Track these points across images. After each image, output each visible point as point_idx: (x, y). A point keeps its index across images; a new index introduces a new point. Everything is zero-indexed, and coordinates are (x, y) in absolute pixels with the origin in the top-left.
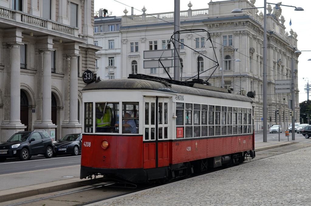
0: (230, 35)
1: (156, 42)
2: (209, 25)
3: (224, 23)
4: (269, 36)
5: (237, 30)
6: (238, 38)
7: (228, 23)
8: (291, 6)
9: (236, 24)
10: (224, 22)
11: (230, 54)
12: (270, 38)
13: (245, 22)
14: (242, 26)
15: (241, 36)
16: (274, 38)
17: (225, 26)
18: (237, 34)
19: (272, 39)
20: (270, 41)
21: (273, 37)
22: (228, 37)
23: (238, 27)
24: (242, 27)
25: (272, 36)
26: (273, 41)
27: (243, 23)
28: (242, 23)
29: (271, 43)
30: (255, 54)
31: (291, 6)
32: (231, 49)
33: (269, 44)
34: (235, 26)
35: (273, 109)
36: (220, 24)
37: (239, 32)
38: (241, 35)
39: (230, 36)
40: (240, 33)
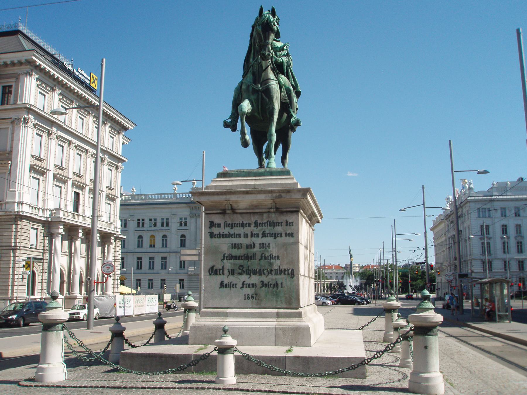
1: (143, 220)
2: (191, 207)
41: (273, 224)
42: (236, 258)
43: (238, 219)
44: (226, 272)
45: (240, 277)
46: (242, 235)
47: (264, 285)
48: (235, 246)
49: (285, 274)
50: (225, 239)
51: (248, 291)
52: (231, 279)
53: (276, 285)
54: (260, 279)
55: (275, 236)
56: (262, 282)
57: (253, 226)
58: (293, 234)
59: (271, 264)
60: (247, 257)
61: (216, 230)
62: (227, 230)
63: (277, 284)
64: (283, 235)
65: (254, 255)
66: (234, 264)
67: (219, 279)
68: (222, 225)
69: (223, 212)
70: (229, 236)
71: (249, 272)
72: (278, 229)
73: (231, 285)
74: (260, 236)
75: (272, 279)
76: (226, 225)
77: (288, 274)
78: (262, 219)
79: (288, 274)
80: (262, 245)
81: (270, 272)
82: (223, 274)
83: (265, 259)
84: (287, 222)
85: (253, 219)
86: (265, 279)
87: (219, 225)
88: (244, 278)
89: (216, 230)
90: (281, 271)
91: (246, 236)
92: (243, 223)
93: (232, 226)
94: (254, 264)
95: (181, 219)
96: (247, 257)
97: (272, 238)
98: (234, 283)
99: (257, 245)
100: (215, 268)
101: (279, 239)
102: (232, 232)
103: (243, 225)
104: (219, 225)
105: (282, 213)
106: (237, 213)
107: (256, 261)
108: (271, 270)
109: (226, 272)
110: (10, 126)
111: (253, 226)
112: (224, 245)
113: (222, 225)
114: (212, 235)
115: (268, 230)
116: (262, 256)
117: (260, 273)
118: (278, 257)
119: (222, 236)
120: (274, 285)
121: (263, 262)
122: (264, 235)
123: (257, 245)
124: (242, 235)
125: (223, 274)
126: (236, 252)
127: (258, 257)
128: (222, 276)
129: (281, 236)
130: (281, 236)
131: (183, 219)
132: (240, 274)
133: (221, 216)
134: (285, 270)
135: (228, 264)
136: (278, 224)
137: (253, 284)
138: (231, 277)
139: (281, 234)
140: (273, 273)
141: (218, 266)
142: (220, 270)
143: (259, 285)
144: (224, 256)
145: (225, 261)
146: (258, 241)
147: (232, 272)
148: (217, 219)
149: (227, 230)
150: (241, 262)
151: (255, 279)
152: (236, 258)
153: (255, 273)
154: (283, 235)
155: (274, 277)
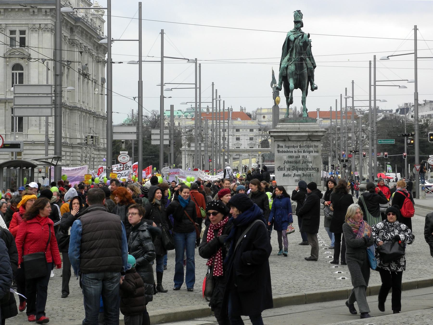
0: (23, 29)
3: (12, 9)
4: (74, 25)
5: (34, 23)
6: (37, 35)
7: (19, 9)
8: (185, 59)
9: (34, 12)
10: (13, 7)
11: (21, 62)
12: (74, 28)
13: (48, 11)
14: (44, 15)
15: (40, 32)
16: (81, 28)
17: (13, 14)
18: (34, 29)
19: (77, 30)
20: (74, 34)
21: (79, 27)
22: (18, 33)
23: (36, 17)
24: (44, 18)
25: (78, 26)
26: (78, 32)
27: (46, 12)
28: (43, 11)
29: (76, 38)
31: (185, 59)
32: (24, 54)
33: (72, 40)
34: (32, 15)
35: (79, 154)
36: (5, 9)
37: (39, 26)
38: (40, 32)
39: (23, 32)
40: (40, 27)
41: (308, 147)
42: (290, 162)
44: (286, 169)
45: (293, 171)
46: (294, 152)
48: (290, 157)
49: (314, 170)
50: (285, 153)
52: (289, 172)
54: (303, 173)
55: (309, 152)
56: (303, 174)
57: (299, 147)
58: (318, 151)
59: (307, 165)
60: (296, 162)
61: (281, 149)
62: (286, 149)
63: (311, 175)
64: (313, 152)
65: (300, 161)
66: (290, 165)
67: (283, 172)
68: (284, 147)
69: (284, 141)
70: (287, 152)
71: (297, 169)
72: (311, 149)
73: (289, 175)
74: (302, 152)
75: (308, 172)
76: (286, 147)
77: (316, 170)
78: (303, 144)
79: (316, 170)
80: (303, 157)
81: (307, 169)
82: (285, 170)
83: (305, 163)
84: (315, 146)
85: (299, 144)
86: (304, 172)
87: (282, 147)
88: (295, 172)
89: (281, 149)
90: (313, 169)
91: (295, 152)
92: (294, 146)
93: (288, 147)
94: (300, 166)
96: (296, 162)
97: (308, 153)
98: (290, 174)
99: (301, 157)
100: (280, 167)
101: (311, 154)
102: (288, 150)
103: (294, 147)
104: (282, 147)
106: (291, 141)
107: (301, 164)
108: (308, 168)
109: (286, 169)
111: (299, 147)
112: (285, 156)
113: (284, 147)
114: (279, 151)
116: (303, 162)
117: (302, 169)
118: (311, 162)
120: (309, 175)
121: (304, 164)
122: (304, 152)
123: (301, 157)
124: (294, 152)
125: (285, 170)
127: (301, 162)
128: (284, 171)
129: (312, 152)
130: (312, 152)
132: (293, 170)
133: (283, 142)
134: (314, 168)
135: (287, 166)
136: (311, 146)
137: (299, 175)
138: (288, 171)
139: (312, 151)
140: (309, 169)
141: (282, 166)
142: (283, 168)
143: (302, 175)
144: (285, 162)
145: (285, 164)
146: (301, 154)
147: (289, 169)
148: (281, 144)
149: (286, 149)
150: (293, 165)
151: (300, 172)
152: (290, 162)
153: (300, 169)
154: (313, 152)
155: (309, 171)
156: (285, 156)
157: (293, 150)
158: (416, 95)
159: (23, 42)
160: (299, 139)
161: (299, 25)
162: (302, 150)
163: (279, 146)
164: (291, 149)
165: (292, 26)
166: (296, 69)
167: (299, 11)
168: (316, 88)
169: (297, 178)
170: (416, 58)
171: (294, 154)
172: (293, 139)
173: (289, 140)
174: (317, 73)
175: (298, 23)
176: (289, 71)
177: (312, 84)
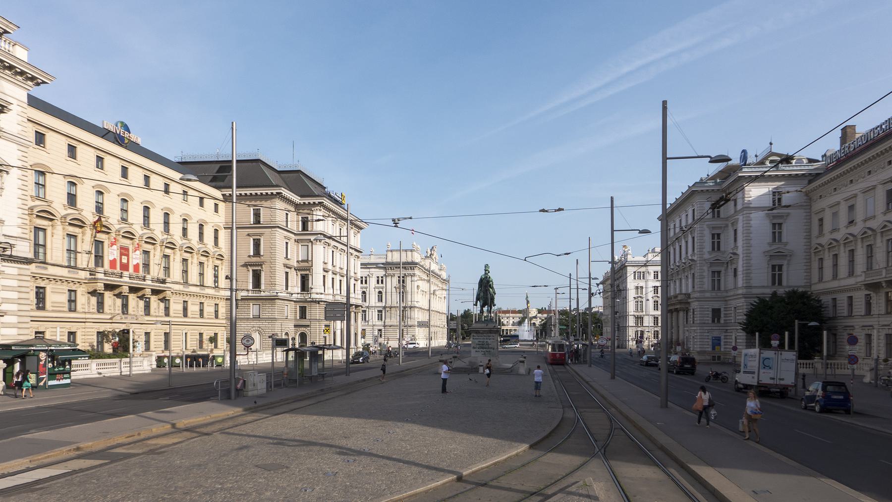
30: (420, 290)
41: (489, 336)
43: (480, 335)
47: (487, 351)
48: (479, 342)
51: (483, 353)
52: (479, 350)
53: (490, 351)
55: (490, 339)
60: (483, 345)
67: (475, 350)
69: (476, 333)
71: (483, 348)
72: (491, 337)
85: (485, 334)
90: (491, 348)
93: (479, 336)
94: (485, 346)
95: (378, 277)
96: (483, 345)
105: (490, 333)
110: (310, 244)
115: (488, 338)
117: (486, 348)
119: (475, 339)
126: (479, 343)
131: (380, 277)
135: (478, 346)
136: (491, 336)
141: (475, 347)
146: (485, 340)
148: (475, 335)
149: (477, 338)
151: (485, 350)
156: (477, 341)
157: (481, 338)
158: (570, 306)
159: (403, 281)
160: (484, 332)
161: (487, 272)
162: (485, 338)
163: (473, 336)
164: (479, 338)
165: (483, 273)
166: (484, 295)
167: (487, 265)
168: (495, 305)
169: (483, 353)
170: (570, 289)
171: (481, 340)
172: (481, 332)
173: (479, 333)
174: (496, 297)
175: (487, 270)
176: (480, 296)
177: (493, 303)
